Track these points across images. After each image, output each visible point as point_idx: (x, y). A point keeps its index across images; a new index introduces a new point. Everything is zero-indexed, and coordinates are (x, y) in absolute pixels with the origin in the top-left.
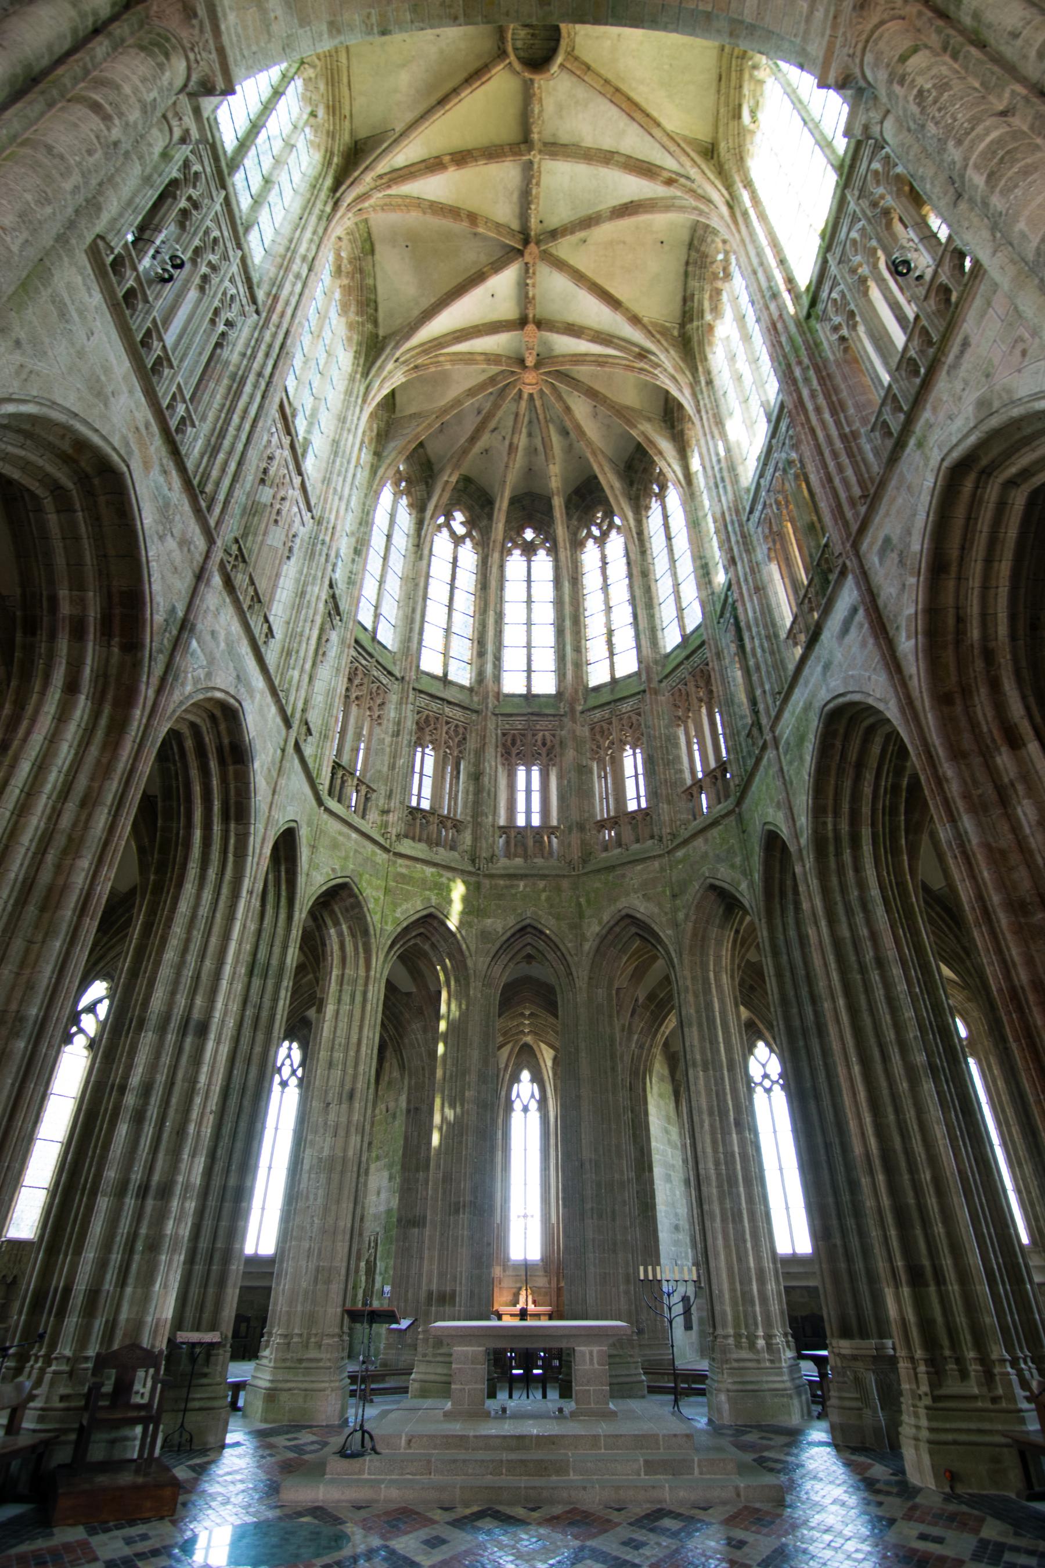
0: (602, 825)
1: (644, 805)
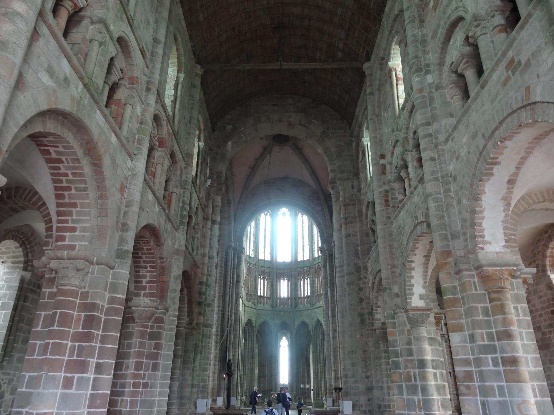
0: (299, 298)
1: (309, 294)
